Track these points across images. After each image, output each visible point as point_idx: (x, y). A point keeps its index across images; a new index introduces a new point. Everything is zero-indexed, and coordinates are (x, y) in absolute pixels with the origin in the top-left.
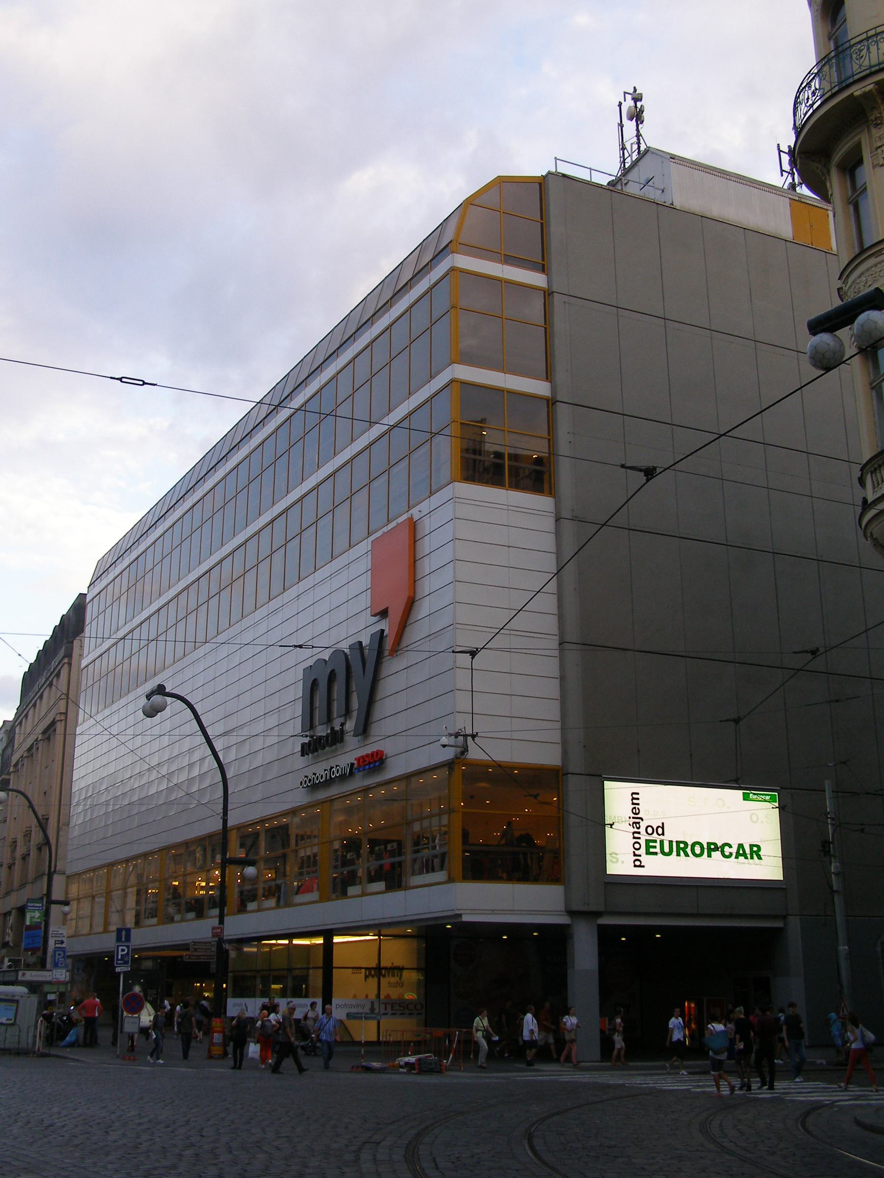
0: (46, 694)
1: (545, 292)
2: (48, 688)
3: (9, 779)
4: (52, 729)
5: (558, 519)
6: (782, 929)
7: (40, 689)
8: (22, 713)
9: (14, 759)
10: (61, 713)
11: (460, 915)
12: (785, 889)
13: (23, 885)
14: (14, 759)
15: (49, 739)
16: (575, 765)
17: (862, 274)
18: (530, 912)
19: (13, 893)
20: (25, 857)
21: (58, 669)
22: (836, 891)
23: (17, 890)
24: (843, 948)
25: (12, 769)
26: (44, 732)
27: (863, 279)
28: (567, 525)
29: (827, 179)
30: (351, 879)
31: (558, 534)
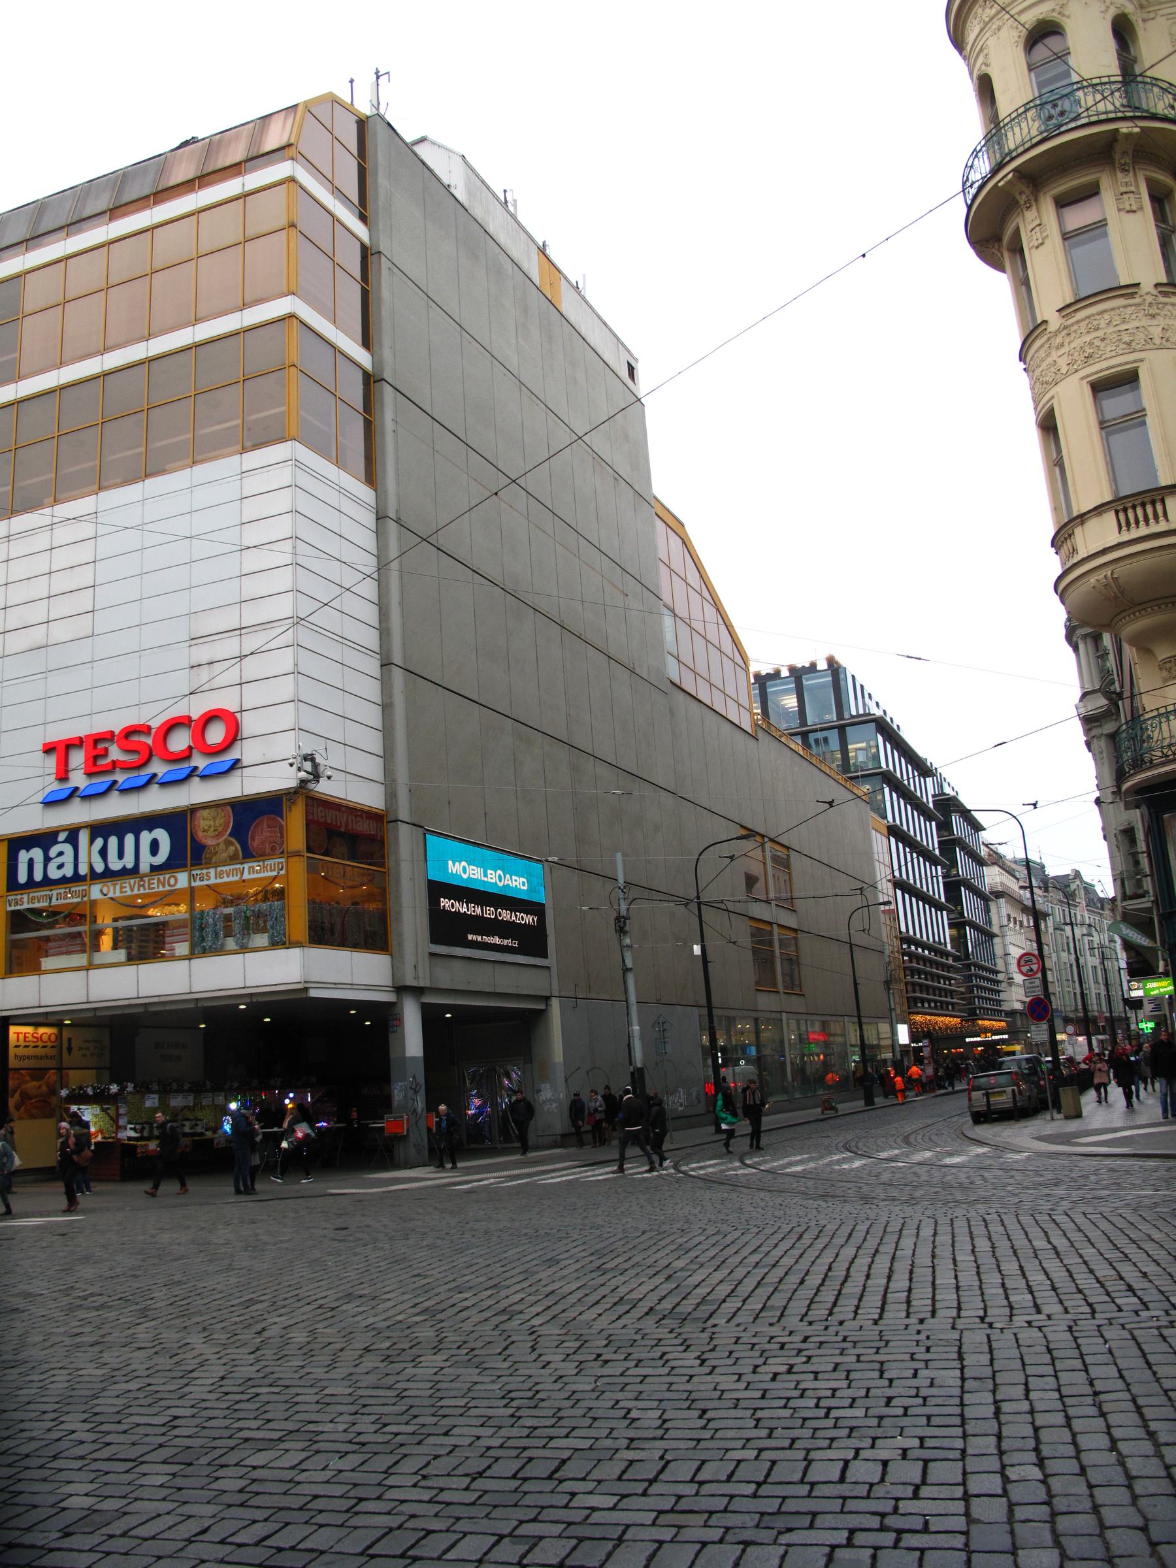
1: (364, 248)
5: (380, 517)
6: (543, 1010)
11: (306, 989)
12: (548, 968)
16: (404, 814)
17: (1105, 311)
18: (368, 987)
22: (631, 969)
24: (636, 1028)
27: (1106, 316)
28: (392, 526)
29: (1034, 208)
30: (43, 948)
31: (380, 533)
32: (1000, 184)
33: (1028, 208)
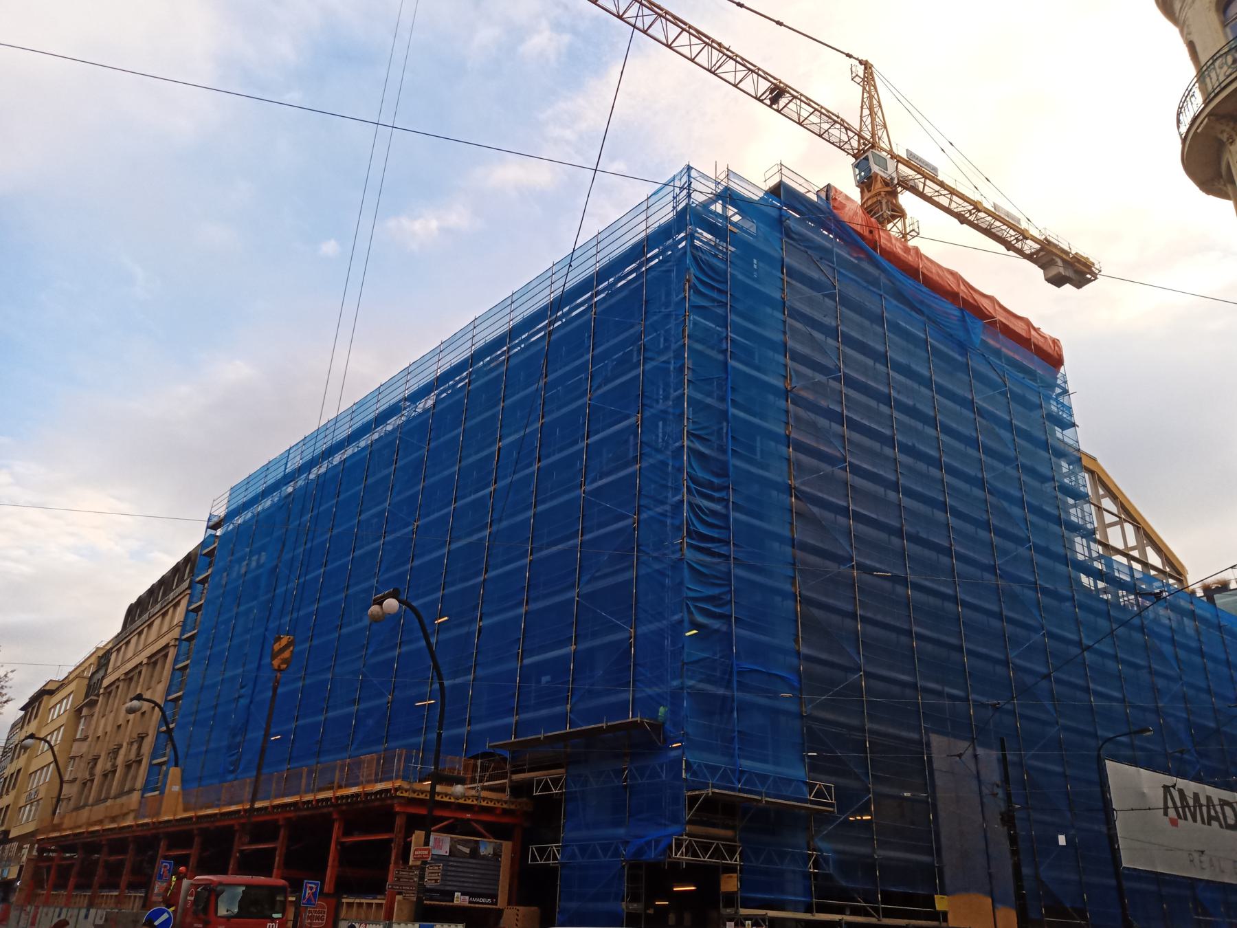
0: (157, 623)
2: (160, 619)
3: (98, 700)
4: (163, 653)
7: (150, 618)
8: (121, 641)
9: (106, 683)
10: (176, 639)
13: (98, 801)
14: (106, 683)
15: (155, 663)
19: (87, 808)
20: (108, 774)
21: (177, 600)
23: (92, 805)
25: (102, 691)
26: (149, 658)
32: (1199, 131)
33: (1231, 143)
